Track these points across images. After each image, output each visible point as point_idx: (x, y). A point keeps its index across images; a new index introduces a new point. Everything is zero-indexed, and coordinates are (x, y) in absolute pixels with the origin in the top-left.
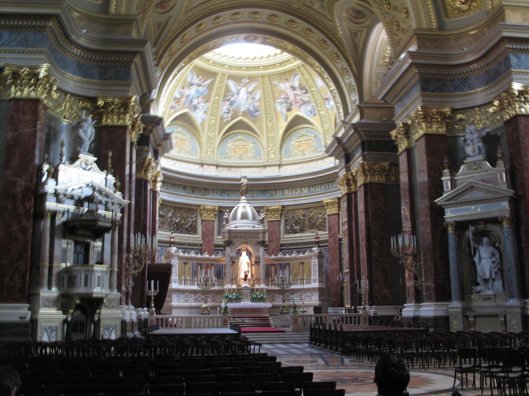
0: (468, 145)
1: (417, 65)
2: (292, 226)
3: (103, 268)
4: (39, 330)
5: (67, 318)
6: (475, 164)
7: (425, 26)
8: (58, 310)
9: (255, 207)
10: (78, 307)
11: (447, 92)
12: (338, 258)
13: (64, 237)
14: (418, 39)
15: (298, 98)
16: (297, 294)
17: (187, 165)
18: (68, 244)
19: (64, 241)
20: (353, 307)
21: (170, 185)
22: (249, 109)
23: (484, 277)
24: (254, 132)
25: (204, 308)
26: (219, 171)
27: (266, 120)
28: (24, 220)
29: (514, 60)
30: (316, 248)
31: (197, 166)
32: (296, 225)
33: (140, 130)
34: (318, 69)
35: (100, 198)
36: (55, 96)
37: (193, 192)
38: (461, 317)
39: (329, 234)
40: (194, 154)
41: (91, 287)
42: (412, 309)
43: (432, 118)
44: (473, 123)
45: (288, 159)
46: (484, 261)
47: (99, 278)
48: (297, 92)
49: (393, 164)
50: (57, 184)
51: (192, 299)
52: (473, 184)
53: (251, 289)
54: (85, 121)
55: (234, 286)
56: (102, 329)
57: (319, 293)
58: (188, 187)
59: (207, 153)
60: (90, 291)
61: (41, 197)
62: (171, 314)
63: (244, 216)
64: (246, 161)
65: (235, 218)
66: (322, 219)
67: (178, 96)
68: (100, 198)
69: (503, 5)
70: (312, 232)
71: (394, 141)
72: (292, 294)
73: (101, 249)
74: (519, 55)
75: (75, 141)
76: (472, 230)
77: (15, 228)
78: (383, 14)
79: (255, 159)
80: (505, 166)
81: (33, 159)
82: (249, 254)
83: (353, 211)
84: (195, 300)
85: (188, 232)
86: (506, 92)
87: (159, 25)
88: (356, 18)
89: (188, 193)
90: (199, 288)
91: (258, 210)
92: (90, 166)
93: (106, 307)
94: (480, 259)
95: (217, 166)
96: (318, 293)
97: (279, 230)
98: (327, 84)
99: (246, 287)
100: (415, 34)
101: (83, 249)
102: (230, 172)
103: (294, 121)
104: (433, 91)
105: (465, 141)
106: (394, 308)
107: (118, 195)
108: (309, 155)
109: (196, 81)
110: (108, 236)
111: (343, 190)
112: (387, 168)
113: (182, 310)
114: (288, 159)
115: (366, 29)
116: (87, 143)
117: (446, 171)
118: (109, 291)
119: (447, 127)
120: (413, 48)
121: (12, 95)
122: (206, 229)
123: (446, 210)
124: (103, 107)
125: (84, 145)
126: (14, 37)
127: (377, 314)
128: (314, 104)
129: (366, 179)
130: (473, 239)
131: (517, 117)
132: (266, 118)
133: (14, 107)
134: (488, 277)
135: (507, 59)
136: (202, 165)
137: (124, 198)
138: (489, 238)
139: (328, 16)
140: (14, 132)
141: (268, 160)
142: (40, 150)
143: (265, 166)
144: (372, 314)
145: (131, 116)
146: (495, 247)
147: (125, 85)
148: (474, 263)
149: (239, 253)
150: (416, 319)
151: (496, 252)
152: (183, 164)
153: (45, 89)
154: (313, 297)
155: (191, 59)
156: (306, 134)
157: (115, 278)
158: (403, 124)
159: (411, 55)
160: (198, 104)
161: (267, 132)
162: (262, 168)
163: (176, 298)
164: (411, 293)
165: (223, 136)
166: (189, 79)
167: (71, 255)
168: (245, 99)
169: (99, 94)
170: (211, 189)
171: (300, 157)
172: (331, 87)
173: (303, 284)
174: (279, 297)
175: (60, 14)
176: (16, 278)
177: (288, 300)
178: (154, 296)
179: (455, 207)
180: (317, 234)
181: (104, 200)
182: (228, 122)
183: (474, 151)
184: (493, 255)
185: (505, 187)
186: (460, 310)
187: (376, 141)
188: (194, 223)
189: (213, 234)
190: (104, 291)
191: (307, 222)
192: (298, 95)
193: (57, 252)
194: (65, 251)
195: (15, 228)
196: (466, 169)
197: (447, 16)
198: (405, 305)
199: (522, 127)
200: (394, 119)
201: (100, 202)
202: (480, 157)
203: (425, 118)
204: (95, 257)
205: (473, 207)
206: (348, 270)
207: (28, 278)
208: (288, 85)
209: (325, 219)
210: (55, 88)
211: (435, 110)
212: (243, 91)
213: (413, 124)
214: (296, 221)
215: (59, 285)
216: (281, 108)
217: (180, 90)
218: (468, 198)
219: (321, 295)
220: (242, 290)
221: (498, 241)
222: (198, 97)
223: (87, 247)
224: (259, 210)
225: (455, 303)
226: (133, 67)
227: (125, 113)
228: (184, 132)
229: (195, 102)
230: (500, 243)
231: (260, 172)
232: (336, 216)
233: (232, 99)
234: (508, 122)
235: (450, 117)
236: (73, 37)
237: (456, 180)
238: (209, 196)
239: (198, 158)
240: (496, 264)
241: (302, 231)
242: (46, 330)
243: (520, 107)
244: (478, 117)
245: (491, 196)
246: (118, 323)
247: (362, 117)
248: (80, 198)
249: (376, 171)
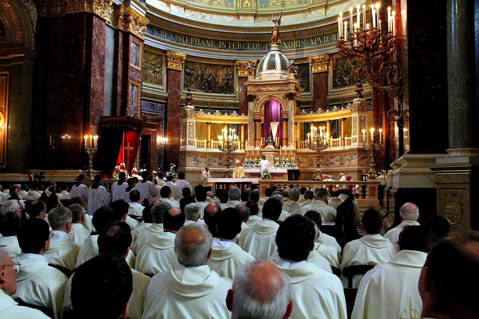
2: (341, 77)
16: (337, 157)
17: (220, 17)
21: (197, 40)
26: (258, 22)
30: (357, 99)
31: (232, 18)
32: (346, 77)
37: (227, 46)
38: (467, 194)
53: (275, 152)
57: (359, 156)
58: (221, 41)
84: (220, 164)
85: (223, 92)
89: (221, 48)
95: (255, 16)
96: (357, 156)
97: (327, 83)
136: (238, 15)
143: (310, 10)
152: (215, 16)
154: (352, 161)
162: (307, 13)
163: (193, 162)
170: (249, 42)
173: (345, 145)
177: (328, 165)
186: (467, 172)
188: (230, 81)
214: (346, 72)
219: (360, 159)
220: (264, 153)
238: (246, 50)
239: (234, 9)
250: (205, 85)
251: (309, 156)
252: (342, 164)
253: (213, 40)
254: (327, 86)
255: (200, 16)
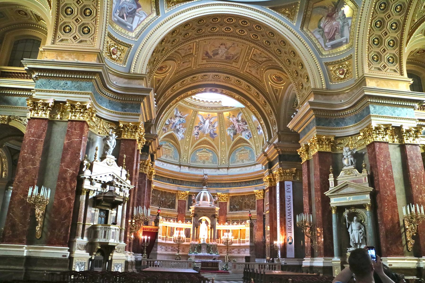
0: (345, 159)
1: (314, 110)
3: (117, 227)
4: (74, 264)
5: (92, 257)
6: (349, 171)
7: (318, 86)
8: (87, 252)
9: (212, 194)
10: (99, 251)
11: (331, 126)
12: (263, 227)
13: (94, 207)
14: (314, 94)
15: (240, 127)
18: (95, 211)
19: (94, 209)
20: (271, 259)
22: (210, 133)
23: (354, 242)
24: (213, 147)
25: (177, 256)
27: (221, 140)
28: (70, 194)
29: (372, 108)
30: (249, 221)
31: (177, 167)
32: (237, 206)
33: (143, 143)
34: (254, 110)
35: (117, 183)
36: (94, 119)
39: (257, 212)
40: (176, 159)
41: (108, 239)
42: (309, 262)
43: (323, 142)
44: (348, 145)
45: (232, 164)
46: (354, 232)
47: (113, 233)
48: (239, 124)
49: (298, 170)
50: (91, 174)
51: (170, 249)
52: (347, 183)
54: (111, 135)
55: (197, 243)
56: (113, 266)
59: (183, 159)
60: (107, 241)
61: (81, 181)
62: (156, 259)
63: (205, 199)
64: (207, 164)
65: (199, 200)
66: (253, 202)
67: (167, 123)
68: (117, 183)
69: (365, 76)
70: (246, 211)
71: (299, 156)
72: (233, 249)
73: (115, 215)
74: (375, 106)
75: (104, 147)
76: (347, 212)
77: (64, 199)
78: (293, 79)
79: (213, 163)
80: (367, 173)
81: (78, 157)
82: (207, 222)
83: (273, 198)
84: (172, 250)
85: (169, 208)
86: (367, 127)
87: (159, 80)
88: (278, 81)
90: (174, 243)
91: (214, 195)
92: (112, 163)
93: (117, 252)
94: (352, 230)
95: (189, 167)
96: (249, 249)
98: (259, 120)
99: (204, 243)
100: (312, 91)
101: (104, 215)
102: (197, 171)
103: (237, 141)
104: (323, 126)
105: (343, 156)
106: (297, 260)
107: (129, 182)
108: (246, 162)
109: (179, 114)
110: (120, 207)
111: (267, 185)
112: (294, 172)
113: (163, 256)
114: (232, 164)
115: (283, 87)
116: (111, 150)
117: (331, 175)
118: (119, 242)
119: (331, 148)
120: (312, 99)
121: (69, 119)
122: (180, 206)
123: (331, 199)
124: (123, 128)
125: (110, 150)
126: (73, 84)
127: (286, 264)
128: (250, 131)
129: (281, 178)
130: (348, 218)
131: (374, 143)
132: (220, 138)
133: (70, 125)
134: (357, 242)
135: (368, 108)
136: (180, 166)
137: (131, 184)
138: (358, 217)
139: (260, 79)
140: (68, 141)
141: (221, 164)
142: (83, 152)
143: (219, 168)
144: (283, 264)
145: (139, 134)
146: (362, 223)
147: (136, 115)
148: (349, 233)
149: (201, 221)
150: (311, 268)
151: (362, 226)
152: (169, 165)
153: (89, 115)
154: (246, 252)
155: (177, 101)
156: (245, 149)
157: (123, 234)
158: (305, 145)
159: (311, 103)
160: (179, 128)
161: (221, 147)
163: (160, 248)
164: (309, 251)
165: (193, 149)
166: (175, 113)
167: (97, 218)
168: (208, 127)
169: (120, 119)
171: (240, 163)
172: (261, 121)
173: (240, 243)
174: (224, 251)
175: (101, 72)
176: (62, 230)
177: (230, 253)
178: (147, 247)
179: (337, 197)
180: (250, 211)
181: (119, 184)
182: (197, 140)
183: (348, 163)
184: (360, 228)
185: (367, 185)
187: (288, 155)
189: (185, 209)
190: (115, 242)
191: (244, 204)
192: (241, 125)
193: (89, 215)
194: (93, 215)
195: (64, 199)
196: (343, 173)
197: (332, 82)
198: (304, 258)
199: (377, 149)
200: (299, 142)
201: (117, 185)
202: (352, 167)
203: (318, 141)
204: (112, 220)
205: (348, 198)
206: (269, 235)
207: (69, 231)
208: (234, 119)
209: (255, 202)
210: (95, 115)
211: (324, 137)
212: (207, 122)
213: (311, 145)
215: (88, 237)
216: (229, 133)
217: (169, 120)
218: (345, 192)
221: (363, 220)
222: (179, 124)
223: (107, 213)
224: (213, 195)
225: (336, 258)
226: (142, 104)
227: (135, 132)
228: (170, 145)
229: (178, 127)
230: (364, 221)
231: (216, 172)
232: (263, 201)
233: (200, 126)
234: (368, 146)
235: (333, 142)
236: (108, 86)
237: (338, 181)
238: (183, 185)
240: (362, 234)
241: (241, 209)
242: (78, 265)
243: (376, 137)
244: (350, 143)
245: (359, 190)
246: (123, 263)
247: (279, 141)
248: (104, 182)
249: (287, 173)
250: (160, 203)
251: (220, 247)
252: (239, 253)
253: (167, 178)
254: (226, 210)
255: (161, 164)
